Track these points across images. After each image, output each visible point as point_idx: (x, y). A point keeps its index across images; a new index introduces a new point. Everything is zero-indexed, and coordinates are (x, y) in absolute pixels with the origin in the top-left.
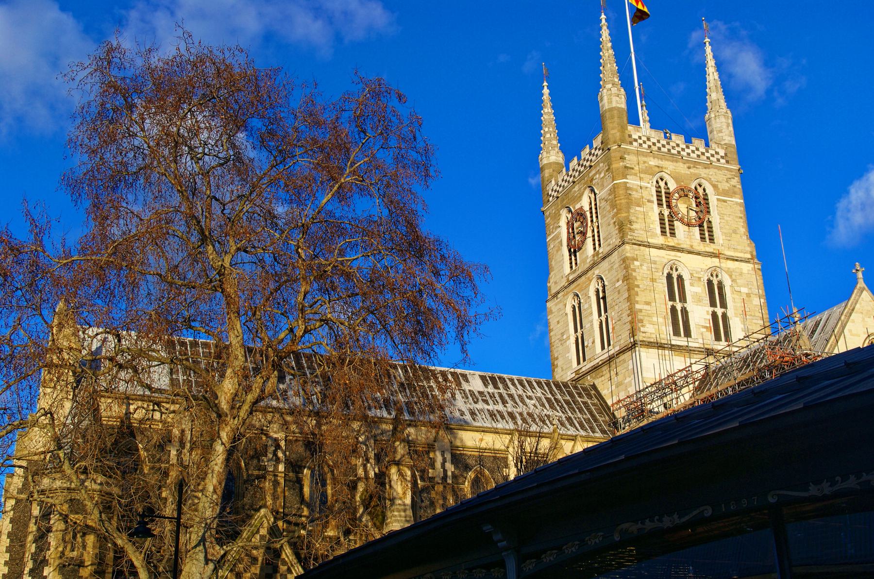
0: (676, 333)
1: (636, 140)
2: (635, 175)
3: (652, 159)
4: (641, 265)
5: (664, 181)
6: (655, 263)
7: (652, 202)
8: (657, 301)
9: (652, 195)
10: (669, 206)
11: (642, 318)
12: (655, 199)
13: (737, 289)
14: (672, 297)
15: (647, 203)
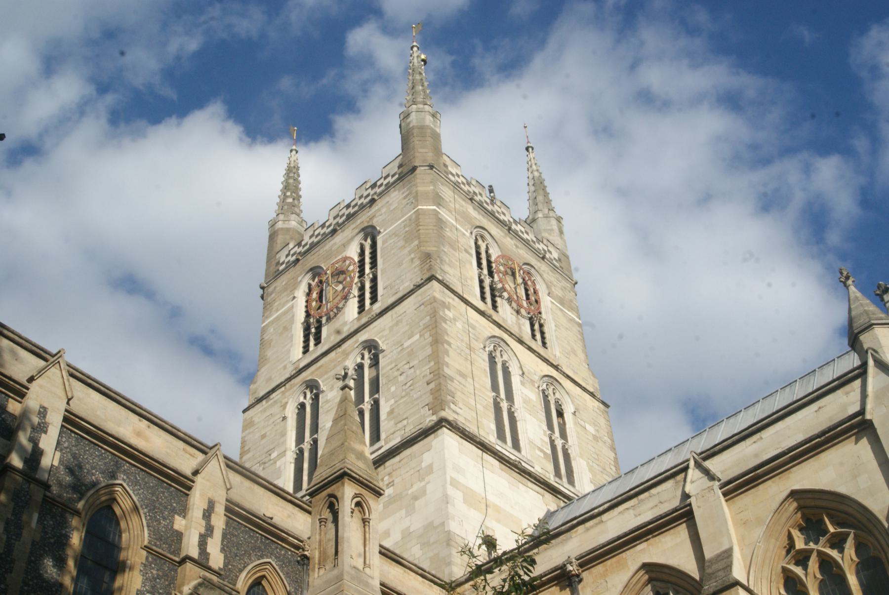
0: (501, 436)
1: (453, 175)
2: (450, 211)
3: (471, 208)
4: (455, 319)
5: (486, 243)
6: (474, 328)
7: (471, 255)
8: (476, 379)
9: (471, 248)
10: (491, 274)
11: (453, 390)
12: (474, 252)
13: (582, 423)
14: (495, 387)
15: (464, 252)
